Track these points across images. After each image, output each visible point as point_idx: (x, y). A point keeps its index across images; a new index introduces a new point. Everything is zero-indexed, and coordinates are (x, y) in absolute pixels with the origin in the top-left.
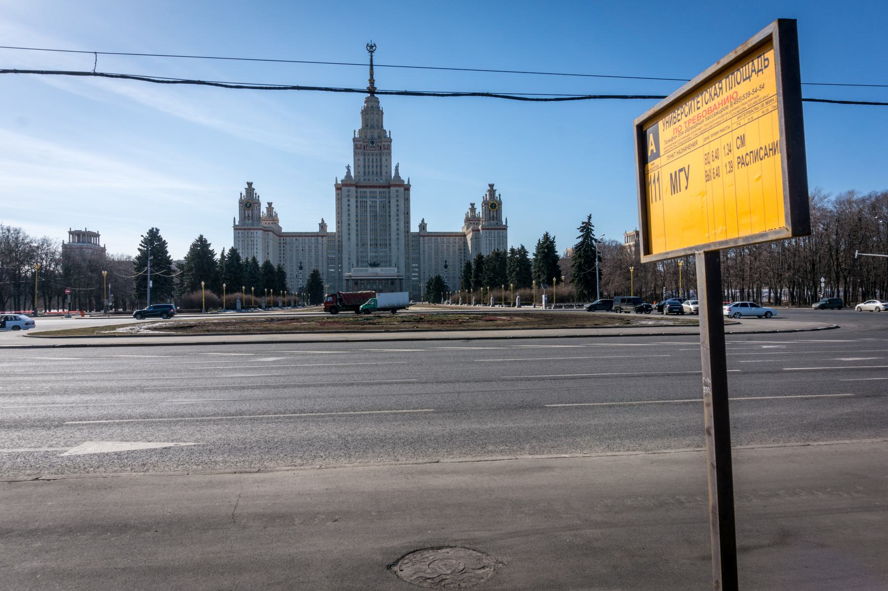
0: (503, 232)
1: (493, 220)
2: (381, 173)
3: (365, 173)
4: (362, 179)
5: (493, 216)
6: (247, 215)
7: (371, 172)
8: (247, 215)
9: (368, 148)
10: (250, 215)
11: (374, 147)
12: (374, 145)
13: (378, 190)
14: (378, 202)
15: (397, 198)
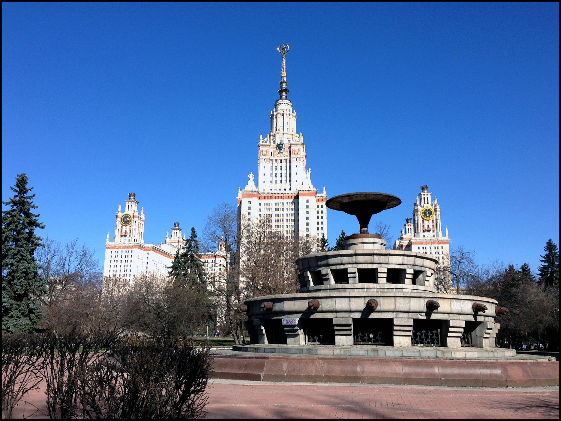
0: (442, 247)
1: (429, 231)
2: (290, 181)
3: (272, 181)
4: (267, 191)
5: (428, 226)
6: (124, 231)
7: (279, 182)
8: (124, 231)
9: (275, 154)
10: (128, 232)
11: (282, 153)
12: (283, 150)
13: (285, 201)
14: (285, 215)
15: (307, 210)
